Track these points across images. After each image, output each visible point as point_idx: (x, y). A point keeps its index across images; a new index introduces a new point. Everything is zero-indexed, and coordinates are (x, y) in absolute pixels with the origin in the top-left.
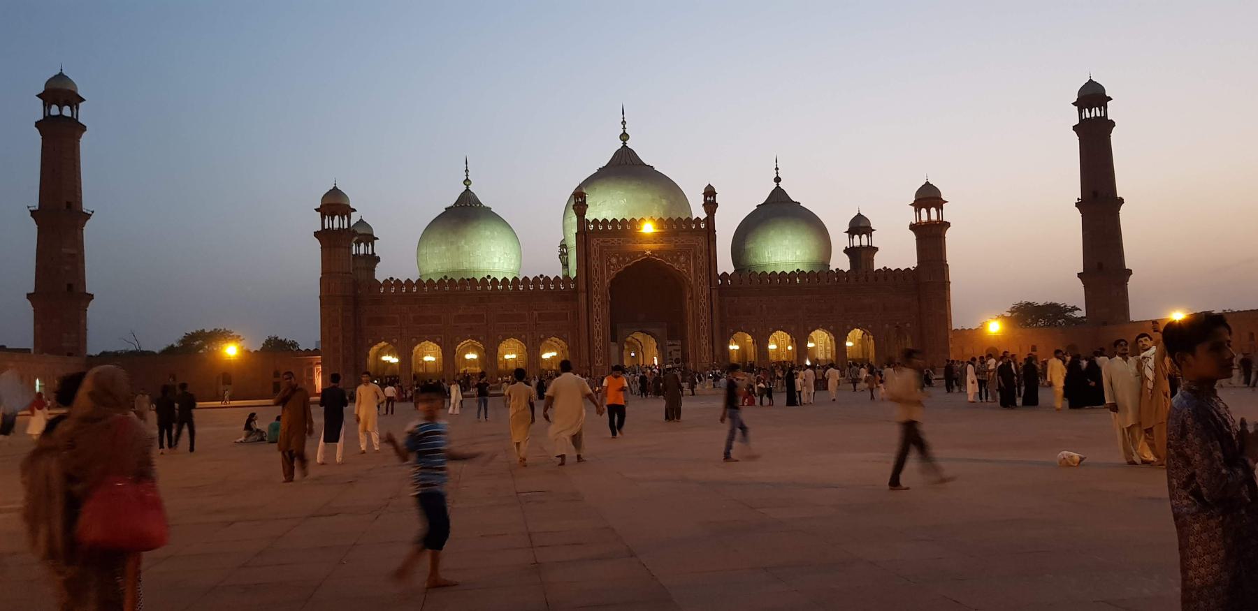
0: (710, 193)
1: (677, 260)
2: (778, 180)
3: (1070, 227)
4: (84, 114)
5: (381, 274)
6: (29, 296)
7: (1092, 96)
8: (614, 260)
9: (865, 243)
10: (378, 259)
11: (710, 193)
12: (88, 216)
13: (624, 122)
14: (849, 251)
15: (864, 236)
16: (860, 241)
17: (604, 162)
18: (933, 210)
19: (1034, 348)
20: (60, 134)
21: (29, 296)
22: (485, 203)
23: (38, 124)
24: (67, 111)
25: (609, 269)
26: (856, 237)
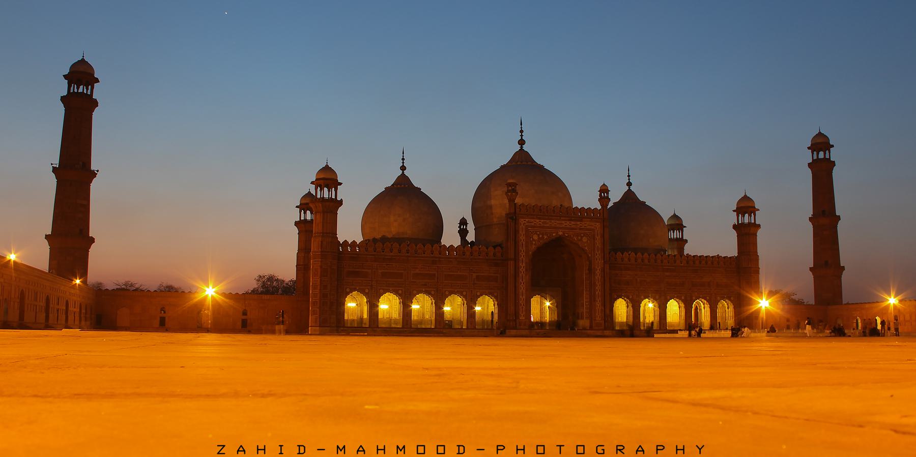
2: (629, 184)
4: (98, 92)
6: (47, 237)
7: (821, 144)
8: (535, 237)
12: (93, 174)
13: (522, 131)
17: (505, 161)
21: (47, 237)
23: (63, 99)
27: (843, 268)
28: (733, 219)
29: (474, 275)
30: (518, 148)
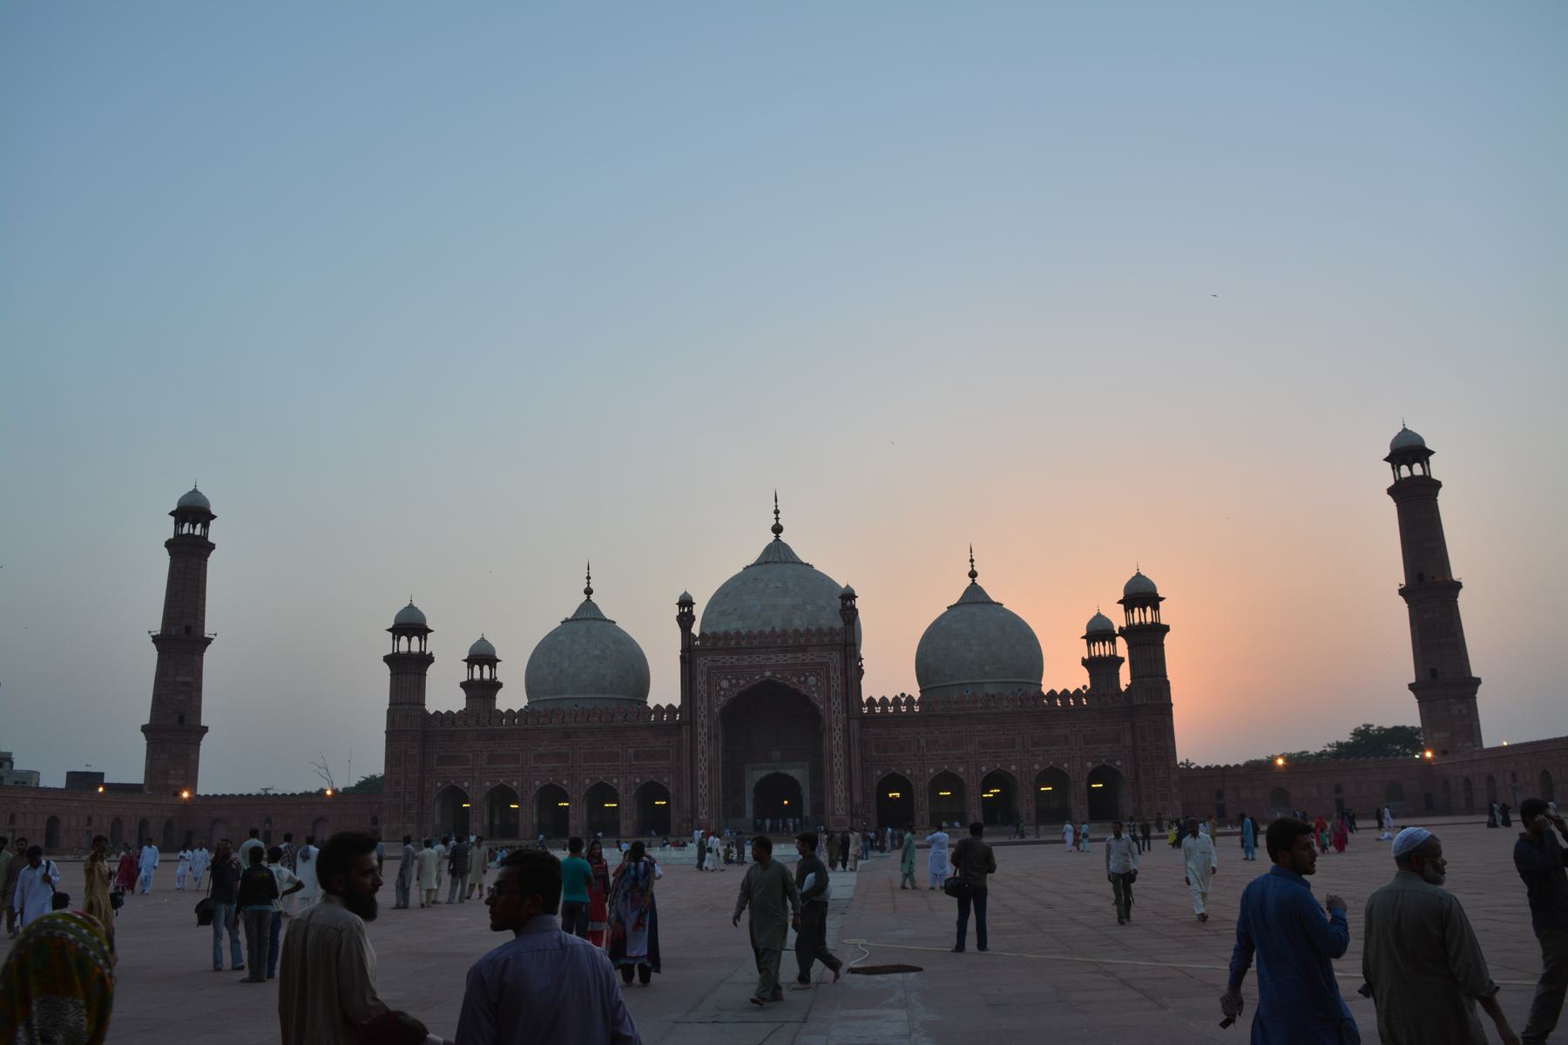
1: (805, 682)
2: (973, 574)
3: (1395, 621)
6: (145, 729)
7: (1408, 450)
8: (725, 684)
10: (500, 685)
12: (209, 641)
13: (777, 512)
14: (1090, 663)
16: (1102, 649)
19: (1338, 789)
20: (189, 554)
21: (145, 729)
23: (169, 544)
27: (1478, 681)
29: (631, 751)
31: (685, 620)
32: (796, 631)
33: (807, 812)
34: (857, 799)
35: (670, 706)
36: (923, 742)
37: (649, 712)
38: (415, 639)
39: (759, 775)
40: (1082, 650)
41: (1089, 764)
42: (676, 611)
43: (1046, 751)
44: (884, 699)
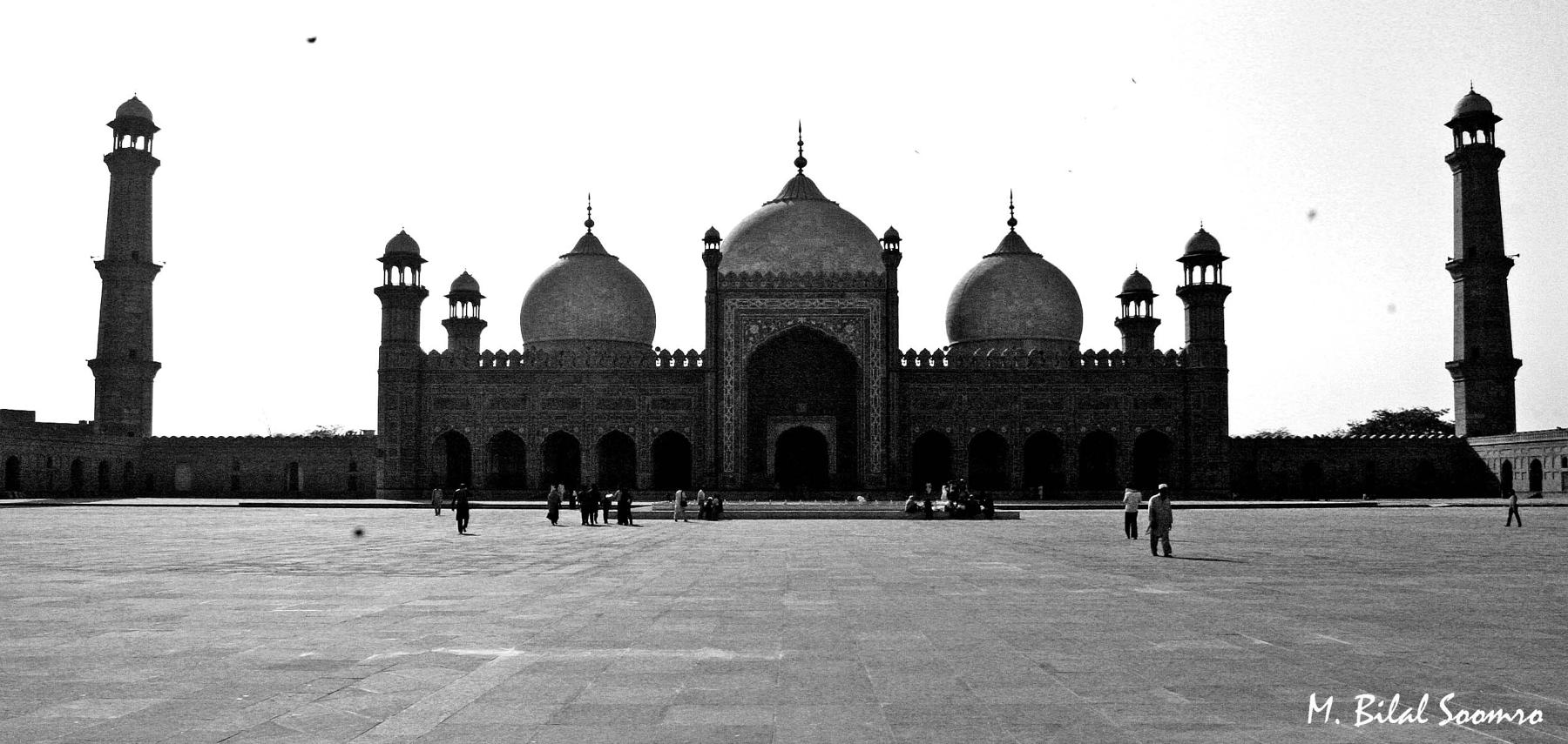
0: (892, 236)
2: (1012, 222)
4: (158, 148)
5: (489, 341)
6: (91, 364)
8: (754, 329)
9: (1143, 313)
10: (484, 324)
11: (892, 236)
12: (158, 268)
13: (800, 143)
14: (1123, 324)
15: (1143, 303)
16: (1137, 310)
18: (1210, 269)
21: (91, 364)
22: (610, 250)
23: (108, 159)
24: (140, 144)
25: (747, 341)
26: (1132, 304)
27: (1519, 363)
28: (1178, 276)
30: (794, 171)
31: (711, 259)
32: (834, 275)
33: (832, 470)
34: (894, 455)
35: (692, 352)
36: (965, 397)
37: (665, 355)
38: (408, 270)
39: (782, 428)
40: (1117, 310)
41: (1138, 430)
42: (702, 247)
43: (1086, 415)
44: (925, 352)
